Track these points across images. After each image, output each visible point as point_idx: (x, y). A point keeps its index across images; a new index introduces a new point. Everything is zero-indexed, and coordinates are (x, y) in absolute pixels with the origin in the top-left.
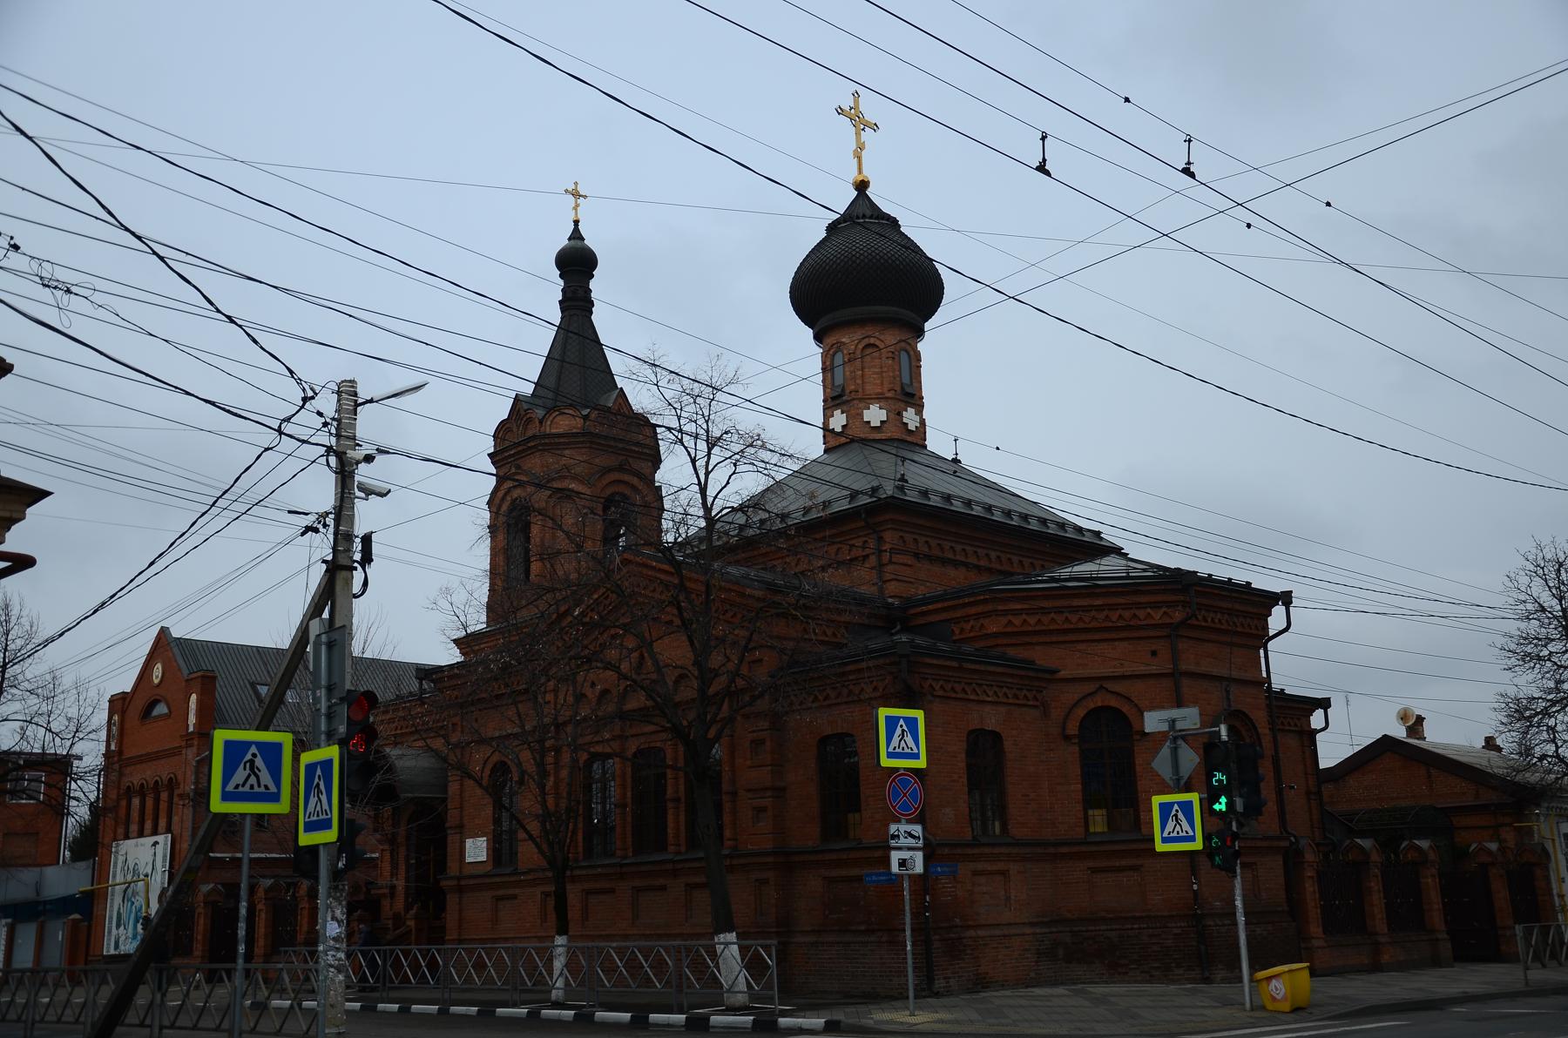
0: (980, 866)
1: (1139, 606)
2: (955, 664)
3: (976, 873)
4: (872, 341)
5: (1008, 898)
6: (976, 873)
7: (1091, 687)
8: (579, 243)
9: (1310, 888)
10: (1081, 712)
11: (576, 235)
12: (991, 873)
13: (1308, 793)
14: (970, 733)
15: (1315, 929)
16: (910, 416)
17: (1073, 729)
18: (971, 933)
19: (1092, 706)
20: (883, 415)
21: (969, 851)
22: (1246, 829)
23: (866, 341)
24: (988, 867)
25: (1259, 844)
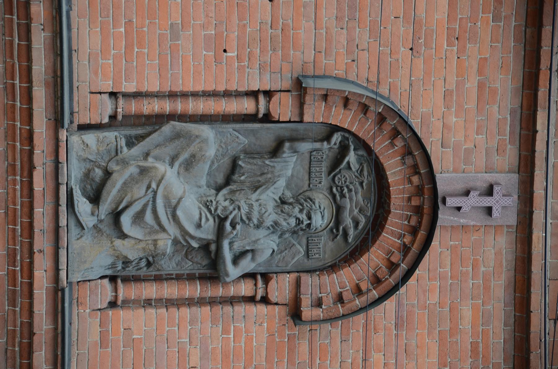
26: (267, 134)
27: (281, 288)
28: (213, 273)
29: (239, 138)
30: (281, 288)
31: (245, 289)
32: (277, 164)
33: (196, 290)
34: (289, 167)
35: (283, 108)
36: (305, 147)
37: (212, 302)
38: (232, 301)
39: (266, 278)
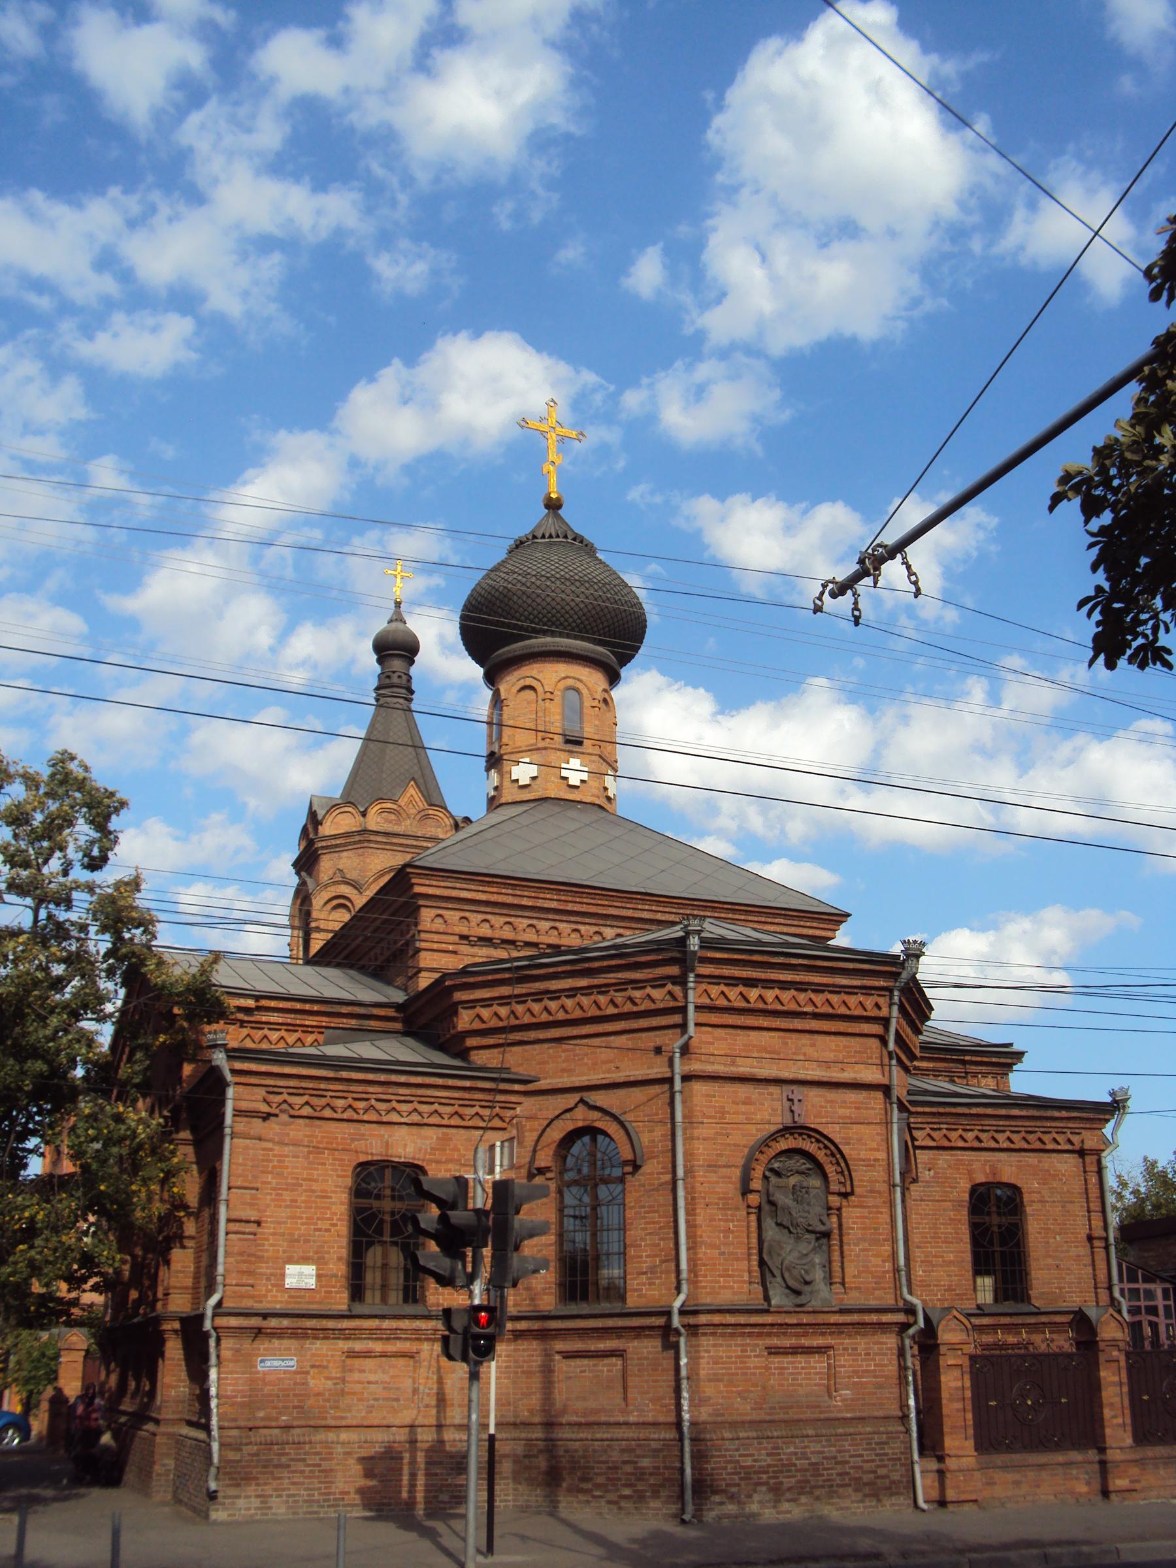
0: (358, 1346)
1: (637, 984)
2: (331, 1074)
3: (352, 1354)
4: (528, 682)
5: (415, 1391)
6: (352, 1354)
7: (571, 1099)
8: (400, 625)
9: (954, 1382)
10: (556, 1134)
11: (398, 618)
12: (384, 1355)
13: (1090, 1238)
14: (361, 1164)
15: (959, 1443)
16: (575, 770)
17: (545, 1159)
18: (321, 1436)
19: (571, 1126)
20: (533, 770)
21: (331, 1324)
22: (802, 1299)
23: (522, 683)
24: (378, 1347)
25: (833, 1319)
26: (766, 1207)
27: (834, 1200)
28: (827, 1235)
29: (769, 1223)
30: (834, 1200)
31: (834, 1219)
32: (780, 1203)
33: (835, 1242)
34: (782, 1199)
35: (754, 1199)
36: (771, 1189)
37: (841, 1235)
38: (840, 1225)
39: (829, 1208)
